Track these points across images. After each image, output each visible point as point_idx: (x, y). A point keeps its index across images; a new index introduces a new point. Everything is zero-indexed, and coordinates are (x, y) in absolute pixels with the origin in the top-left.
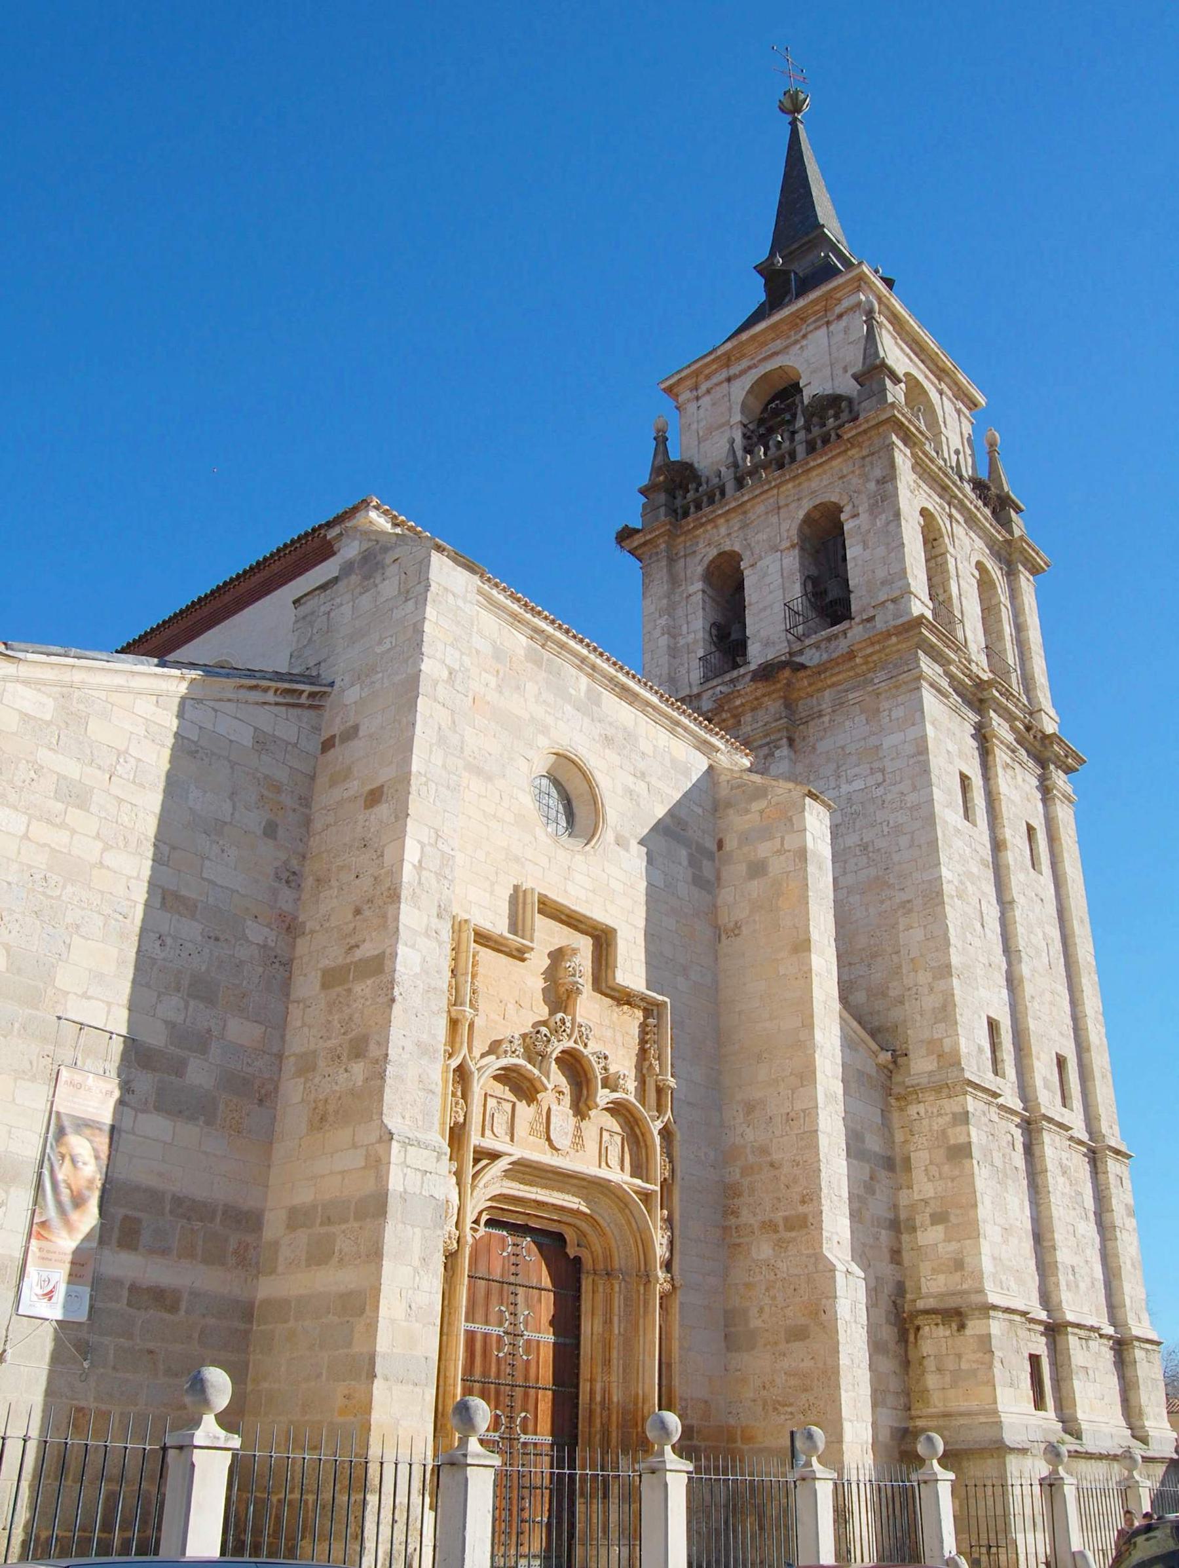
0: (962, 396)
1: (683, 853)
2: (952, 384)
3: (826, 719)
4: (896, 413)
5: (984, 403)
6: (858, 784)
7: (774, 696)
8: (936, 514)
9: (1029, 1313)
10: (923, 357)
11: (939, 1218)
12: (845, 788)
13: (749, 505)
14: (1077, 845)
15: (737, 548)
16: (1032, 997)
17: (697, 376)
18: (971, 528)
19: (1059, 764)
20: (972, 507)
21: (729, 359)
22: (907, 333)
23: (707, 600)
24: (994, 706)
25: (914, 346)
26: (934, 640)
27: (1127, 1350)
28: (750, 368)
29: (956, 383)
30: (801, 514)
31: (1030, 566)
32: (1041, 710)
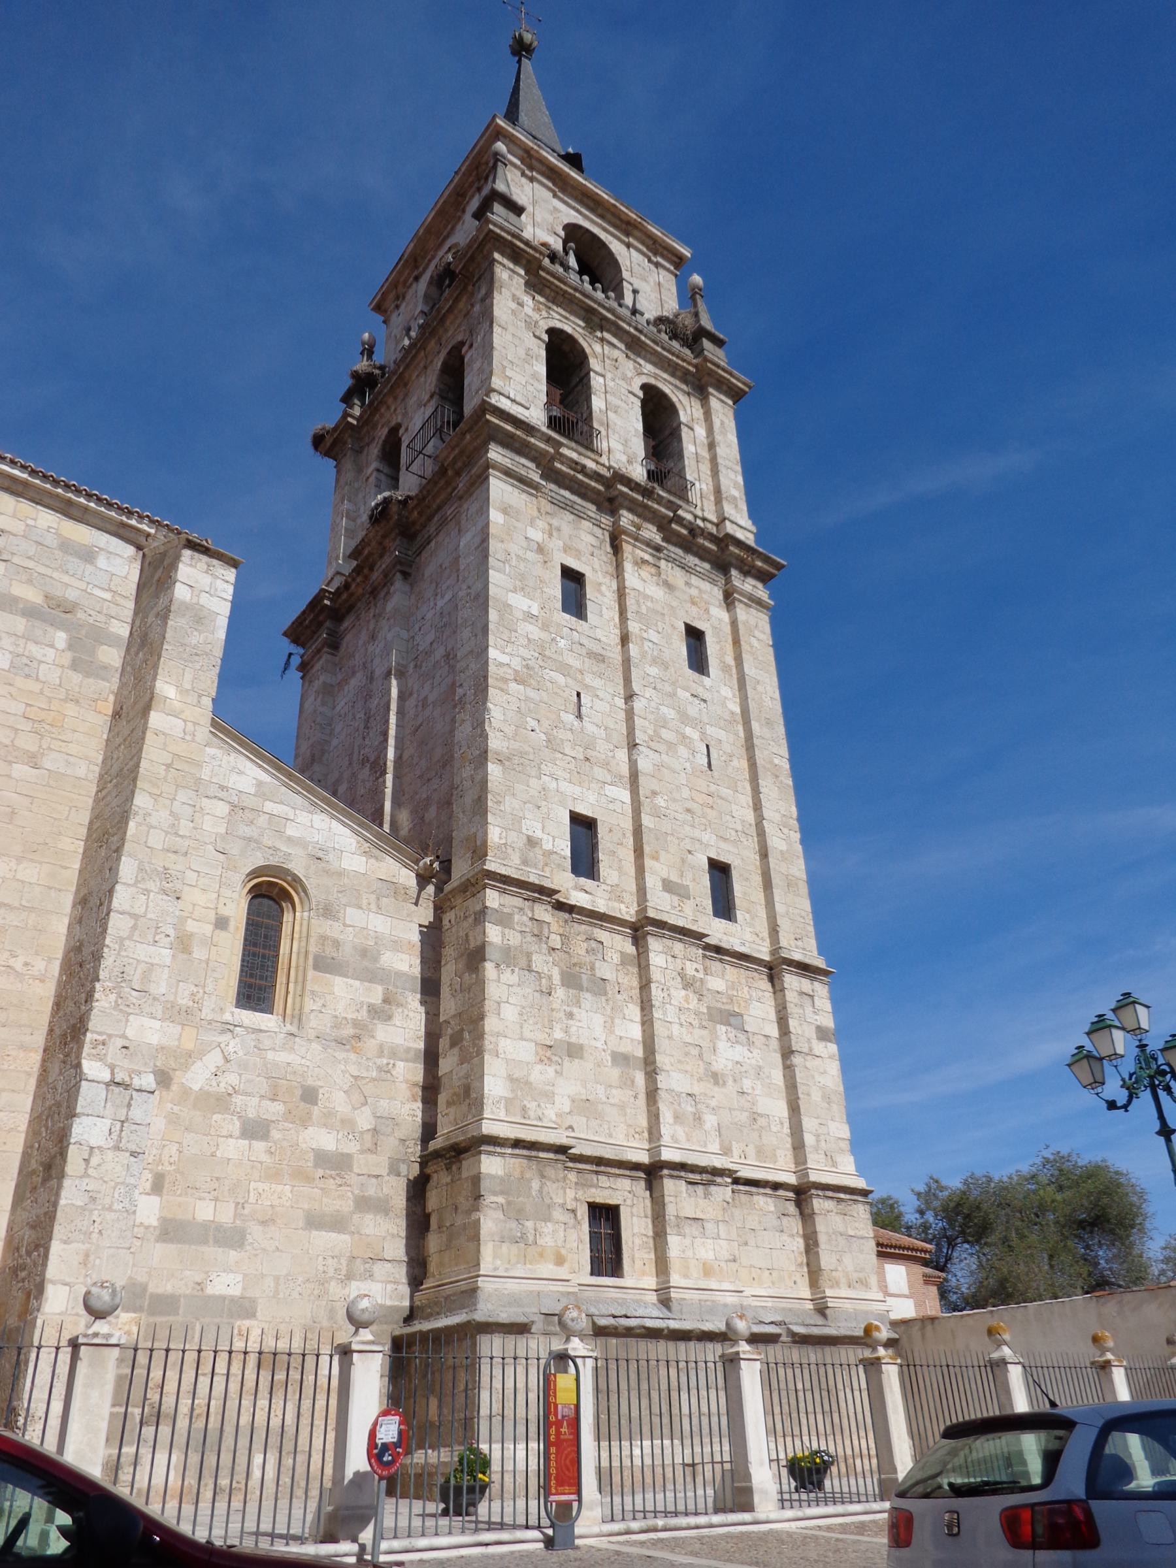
0: (661, 250)
1: (61, 638)
2: (644, 237)
3: (433, 544)
4: (491, 227)
5: (689, 255)
6: (447, 597)
7: (393, 535)
8: (576, 336)
9: (570, 1148)
10: (600, 211)
11: (456, 1041)
12: (440, 603)
13: (406, 375)
14: (771, 649)
15: (399, 420)
16: (654, 793)
17: (396, 287)
18: (639, 355)
19: (746, 568)
20: (632, 330)
21: (416, 260)
22: (573, 187)
23: (383, 477)
24: (626, 503)
25: (585, 200)
26: (509, 428)
27: (806, 1200)
28: (430, 261)
29: (650, 236)
30: (440, 364)
31: (725, 388)
32: (725, 519)
